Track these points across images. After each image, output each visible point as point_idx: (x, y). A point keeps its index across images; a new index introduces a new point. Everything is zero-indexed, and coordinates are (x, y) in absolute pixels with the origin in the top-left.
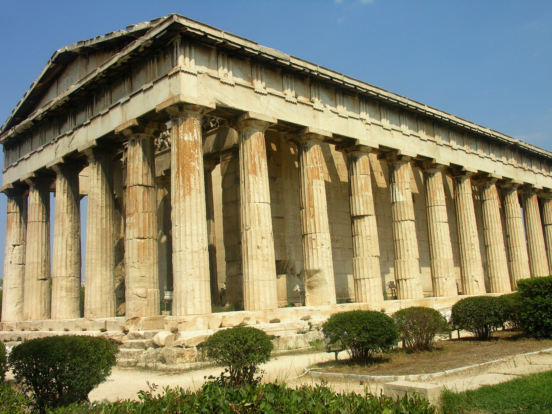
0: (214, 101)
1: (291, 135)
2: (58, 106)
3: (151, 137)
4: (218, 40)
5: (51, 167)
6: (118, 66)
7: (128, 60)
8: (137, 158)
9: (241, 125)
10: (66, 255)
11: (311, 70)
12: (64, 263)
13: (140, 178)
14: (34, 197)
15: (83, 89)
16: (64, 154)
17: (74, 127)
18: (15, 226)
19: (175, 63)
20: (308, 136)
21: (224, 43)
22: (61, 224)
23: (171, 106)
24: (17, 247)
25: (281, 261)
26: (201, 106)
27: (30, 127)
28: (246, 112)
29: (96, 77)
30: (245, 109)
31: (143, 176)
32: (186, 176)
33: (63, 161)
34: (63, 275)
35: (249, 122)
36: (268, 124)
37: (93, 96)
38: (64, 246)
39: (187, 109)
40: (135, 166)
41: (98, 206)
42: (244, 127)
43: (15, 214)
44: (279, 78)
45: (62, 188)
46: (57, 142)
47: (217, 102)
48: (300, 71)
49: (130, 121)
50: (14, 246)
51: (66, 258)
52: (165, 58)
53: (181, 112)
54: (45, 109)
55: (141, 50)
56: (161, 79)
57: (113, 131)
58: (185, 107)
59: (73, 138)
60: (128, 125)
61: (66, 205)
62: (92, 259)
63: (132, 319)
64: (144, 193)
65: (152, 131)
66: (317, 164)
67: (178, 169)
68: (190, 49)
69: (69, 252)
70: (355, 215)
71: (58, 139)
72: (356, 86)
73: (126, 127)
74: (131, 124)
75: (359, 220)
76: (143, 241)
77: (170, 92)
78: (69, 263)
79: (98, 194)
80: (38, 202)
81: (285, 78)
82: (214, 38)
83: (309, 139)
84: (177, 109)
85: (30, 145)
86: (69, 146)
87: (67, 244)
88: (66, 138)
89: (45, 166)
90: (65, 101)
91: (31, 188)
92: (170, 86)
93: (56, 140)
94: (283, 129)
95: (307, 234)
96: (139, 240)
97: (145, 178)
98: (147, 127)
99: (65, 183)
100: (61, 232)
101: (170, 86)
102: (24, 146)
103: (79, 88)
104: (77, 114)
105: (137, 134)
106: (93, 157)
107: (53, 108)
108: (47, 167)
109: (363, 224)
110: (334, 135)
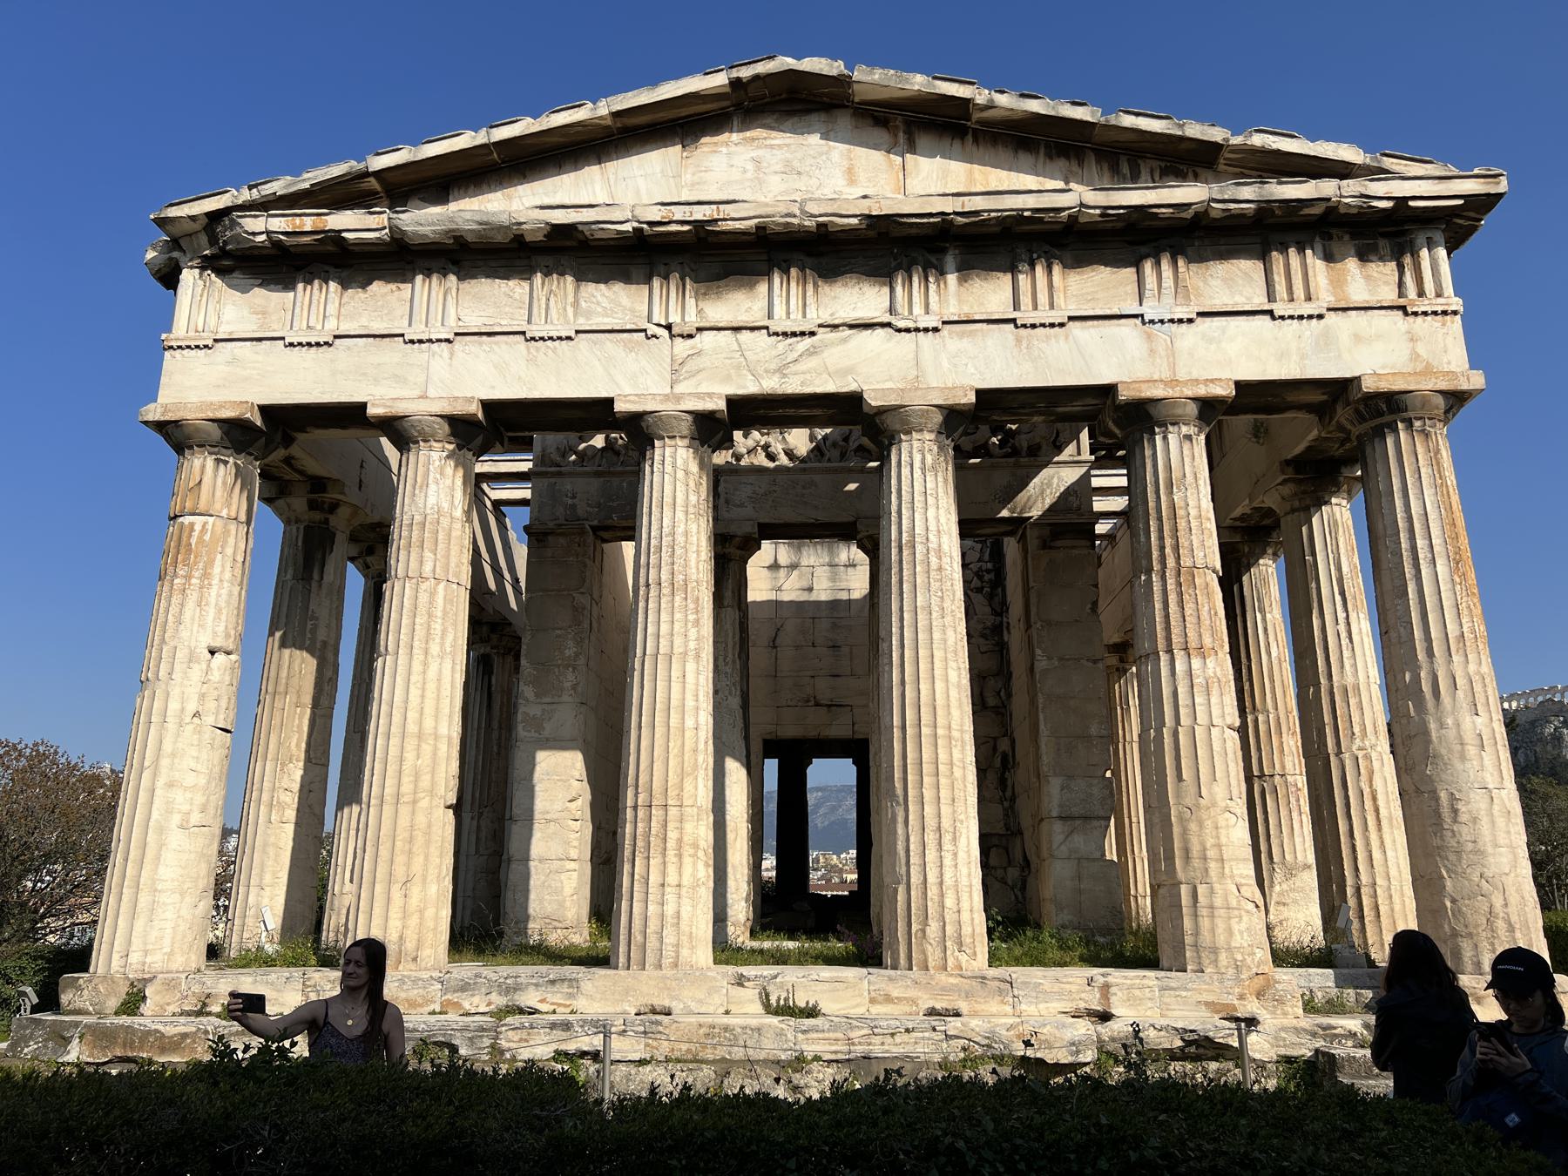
2: (760, 228)
6: (1183, 215)
16: (749, 387)
18: (227, 575)
22: (691, 617)
24: (220, 657)
37: (944, 251)
43: (233, 527)
49: (1212, 381)
50: (212, 653)
54: (679, 213)
55: (1306, 211)
59: (812, 352)
60: (1202, 391)
71: (699, 329)
73: (1190, 393)
77: (1415, 356)
86: (780, 371)
89: (610, 402)
100: (692, 645)
102: (377, 287)
103: (943, 213)
106: (932, 436)
108: (619, 407)
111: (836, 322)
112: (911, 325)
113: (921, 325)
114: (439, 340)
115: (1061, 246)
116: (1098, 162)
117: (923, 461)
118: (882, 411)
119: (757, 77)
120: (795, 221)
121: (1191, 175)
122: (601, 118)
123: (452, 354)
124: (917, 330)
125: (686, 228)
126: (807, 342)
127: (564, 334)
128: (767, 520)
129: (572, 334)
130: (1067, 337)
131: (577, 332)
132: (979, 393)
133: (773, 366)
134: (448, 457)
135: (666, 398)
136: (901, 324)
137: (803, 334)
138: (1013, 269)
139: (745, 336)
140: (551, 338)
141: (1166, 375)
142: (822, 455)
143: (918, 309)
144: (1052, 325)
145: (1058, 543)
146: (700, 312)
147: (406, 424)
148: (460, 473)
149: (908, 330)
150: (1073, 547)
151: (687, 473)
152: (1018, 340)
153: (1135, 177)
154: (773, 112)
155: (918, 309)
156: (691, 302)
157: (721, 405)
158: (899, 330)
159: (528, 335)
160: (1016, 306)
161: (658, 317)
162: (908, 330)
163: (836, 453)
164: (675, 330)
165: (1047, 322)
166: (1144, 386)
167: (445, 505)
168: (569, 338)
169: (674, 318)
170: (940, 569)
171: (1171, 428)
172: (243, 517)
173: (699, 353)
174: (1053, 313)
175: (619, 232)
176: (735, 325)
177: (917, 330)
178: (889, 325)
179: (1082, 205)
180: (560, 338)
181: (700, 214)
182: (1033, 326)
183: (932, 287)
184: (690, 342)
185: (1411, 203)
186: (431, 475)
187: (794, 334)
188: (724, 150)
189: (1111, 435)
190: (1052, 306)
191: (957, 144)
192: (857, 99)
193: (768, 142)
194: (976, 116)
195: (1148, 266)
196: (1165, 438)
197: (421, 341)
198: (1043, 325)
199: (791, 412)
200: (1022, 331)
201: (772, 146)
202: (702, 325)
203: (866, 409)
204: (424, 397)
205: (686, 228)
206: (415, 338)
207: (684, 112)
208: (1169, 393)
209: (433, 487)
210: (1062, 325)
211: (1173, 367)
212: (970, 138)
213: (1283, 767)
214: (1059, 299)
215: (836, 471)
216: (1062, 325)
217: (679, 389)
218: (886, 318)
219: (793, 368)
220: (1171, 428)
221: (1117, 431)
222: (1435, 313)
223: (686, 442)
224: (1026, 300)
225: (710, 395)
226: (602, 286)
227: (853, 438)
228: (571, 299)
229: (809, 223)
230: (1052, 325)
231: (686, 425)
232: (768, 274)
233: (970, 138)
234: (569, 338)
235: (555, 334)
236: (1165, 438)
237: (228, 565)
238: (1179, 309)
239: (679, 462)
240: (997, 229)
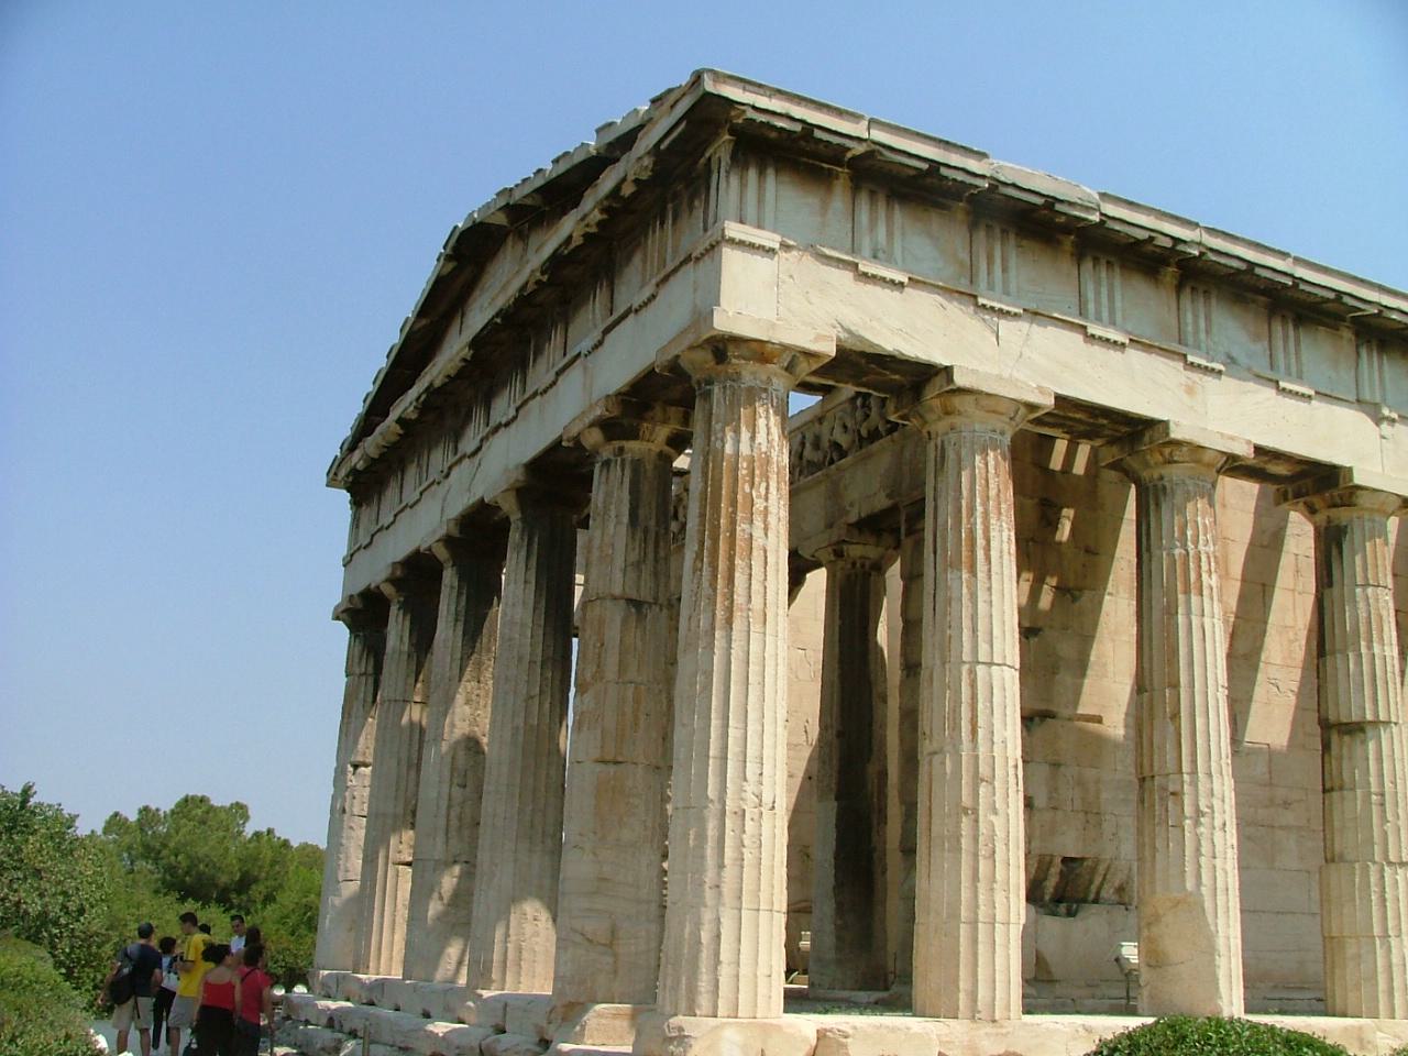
0: (834, 333)
1: (1115, 449)
3: (661, 455)
4: (848, 143)
5: (430, 549)
7: (600, 224)
8: (613, 514)
9: (931, 410)
10: (450, 800)
11: (1177, 240)
12: (442, 822)
13: (618, 575)
14: (397, 631)
17: (484, 431)
19: (711, 220)
20: (1167, 451)
21: (870, 154)
23: (691, 348)
25: (1083, 859)
26: (785, 348)
27: (394, 438)
28: (948, 370)
30: (940, 359)
31: (625, 572)
32: (662, 553)
33: (455, 533)
34: (437, 858)
35: (957, 401)
36: (1023, 410)
38: (447, 773)
39: (735, 357)
40: (606, 539)
41: (520, 659)
42: (940, 419)
43: (364, 678)
44: (1067, 265)
45: (453, 608)
46: (447, 476)
47: (843, 335)
48: (1138, 242)
51: (449, 807)
52: (691, 208)
53: (720, 367)
55: (628, 190)
56: (675, 270)
57: (559, 442)
58: (731, 351)
61: (459, 656)
62: (495, 816)
63: (565, 1006)
64: (625, 622)
65: (663, 432)
66: (1196, 543)
67: (702, 543)
68: (762, 173)
69: (456, 791)
70: (1332, 718)
71: (450, 468)
72: (1340, 294)
73: (587, 421)
74: (598, 412)
75: (1346, 738)
76: (612, 769)
78: (454, 822)
79: (523, 625)
80: (406, 648)
81: (1088, 265)
82: (835, 140)
83: (1170, 462)
84: (710, 356)
85: (397, 491)
87: (453, 770)
88: (466, 462)
90: (464, 360)
91: (394, 609)
92: (695, 290)
93: (446, 471)
94: (1082, 428)
95: (1153, 777)
96: (602, 765)
97: (631, 574)
98: (646, 420)
99: (459, 594)
101: (695, 290)
105: (617, 444)
106: (520, 516)
108: (422, 550)
109: (1358, 749)
110: (1259, 450)
119: (455, 249)
126: (480, 455)
134: (399, 609)
136: (504, 421)
148: (408, 617)
151: (452, 587)
170: (510, 640)
172: (370, 670)
185: (662, 147)
200: (546, 396)
213: (1152, 766)
222: (707, 250)
237: (361, 708)
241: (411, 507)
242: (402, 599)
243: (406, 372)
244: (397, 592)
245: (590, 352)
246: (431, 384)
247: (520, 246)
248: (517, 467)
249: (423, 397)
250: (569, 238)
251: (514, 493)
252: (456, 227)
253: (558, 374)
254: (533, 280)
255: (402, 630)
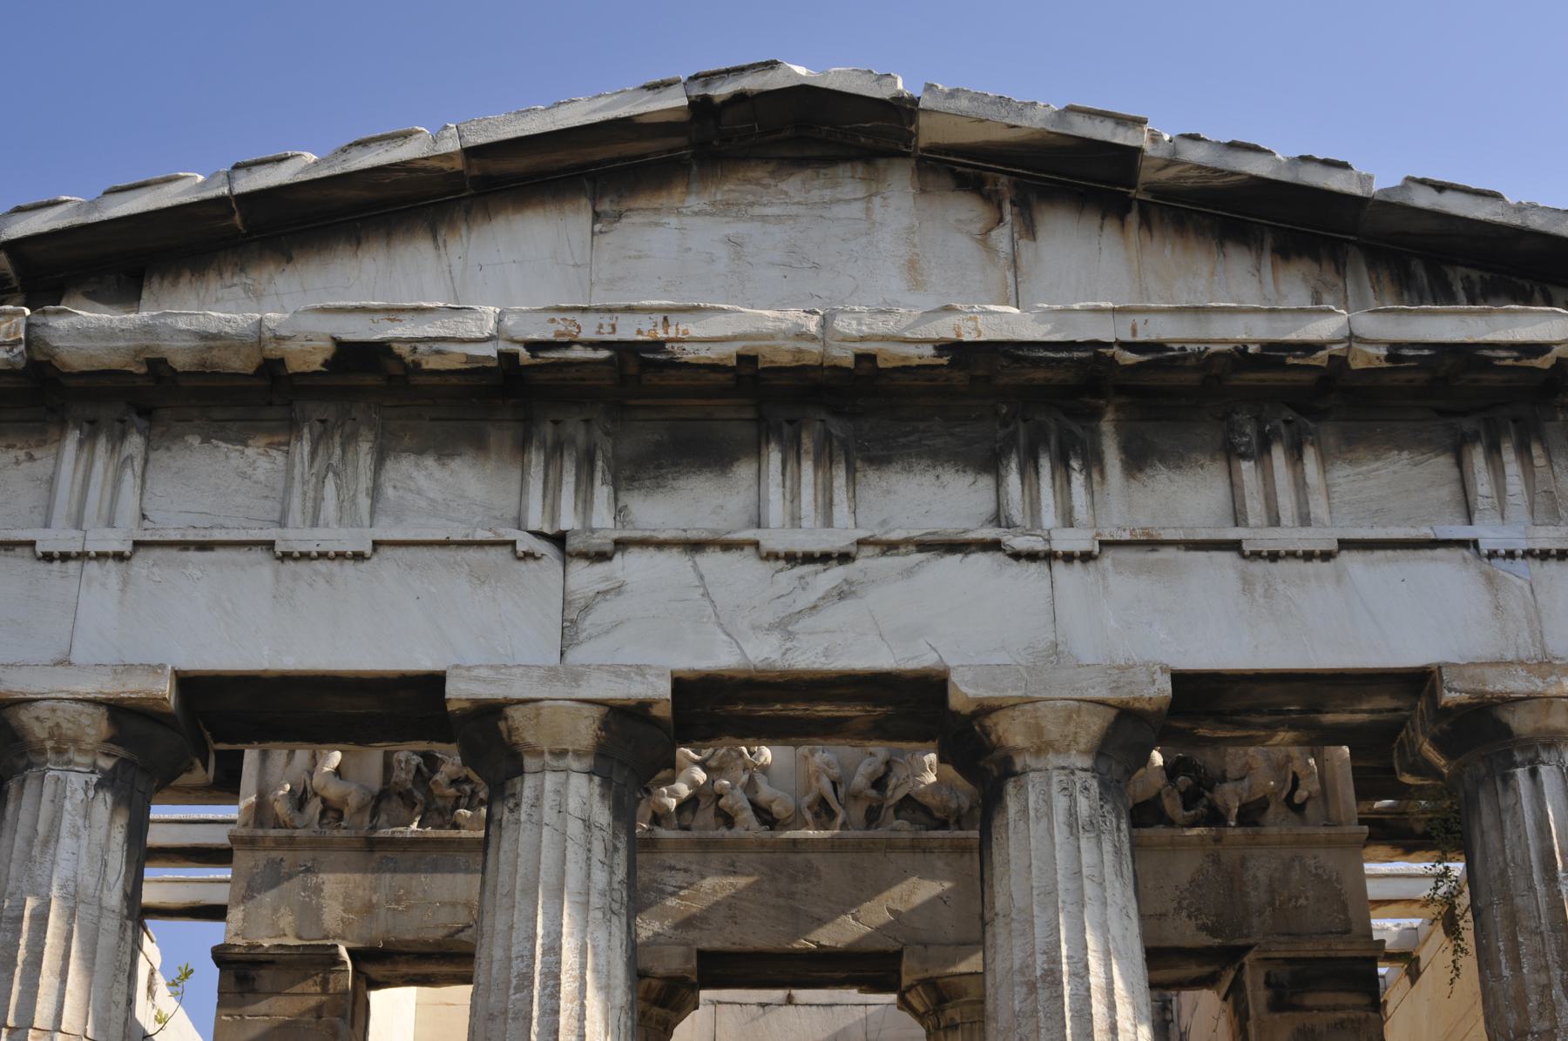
2: (747, 360)
15: (1130, 358)
16: (720, 657)
29: (1310, 348)
37: (1097, 415)
54: (589, 329)
59: (842, 594)
71: (621, 545)
85: (130, 481)
89: (435, 681)
93: (602, 541)
104: (881, 460)
106: (1087, 762)
107: (691, 354)
108: (458, 691)
111: (895, 535)
112: (1039, 545)
113: (1060, 546)
114: (101, 556)
115: (1319, 415)
116: (1372, 266)
117: (1072, 812)
118: (986, 710)
119: (740, 98)
120: (815, 348)
121: (1537, 296)
122: (448, 156)
123: (125, 582)
124: (1049, 557)
125: (603, 354)
126: (835, 574)
127: (349, 549)
128: (717, 944)
129: (368, 549)
130: (1339, 579)
131: (377, 544)
132: (1181, 679)
133: (768, 618)
134: (99, 786)
135: (552, 674)
136: (1021, 543)
137: (825, 558)
138: (1231, 453)
139: (711, 561)
140: (322, 556)
141: (1529, 651)
142: (832, 814)
143: (1049, 517)
144: (1308, 556)
145: (1310, 1000)
146: (620, 512)
147: (25, 716)
149: (1032, 556)
150: (1335, 1009)
151: (588, 824)
152: (1247, 583)
153: (1442, 293)
154: (765, 160)
155: (1049, 517)
156: (602, 493)
157: (664, 690)
158: (1017, 556)
159: (279, 549)
160: (1238, 516)
161: (536, 520)
162: (1032, 556)
163: (858, 812)
164: (573, 544)
165: (1301, 547)
166: (1490, 673)
167: (89, 881)
168: (358, 556)
169: (568, 521)
171: (1544, 756)
173: (619, 590)
174: (1306, 532)
175: (470, 358)
176: (693, 535)
177: (1049, 557)
178: (994, 546)
179: (1352, 337)
180: (340, 556)
181: (628, 329)
182: (1274, 556)
183: (1078, 480)
184: (601, 569)
186: (67, 820)
187: (809, 558)
188: (673, 221)
189: (1423, 768)
190: (1305, 520)
191: (1111, 228)
192: (924, 140)
193: (757, 210)
194: (1146, 175)
195: (1477, 458)
196: (1534, 774)
197: (65, 557)
198: (1292, 555)
199: (798, 709)
201: (764, 218)
202: (626, 534)
203: (954, 702)
204: (65, 662)
205: (603, 354)
206: (56, 548)
207: (600, 153)
208: (1537, 686)
209: (66, 843)
210: (1326, 556)
211: (1539, 636)
212: (1133, 218)
214: (1318, 507)
215: (859, 846)
216: (1326, 556)
217: (576, 656)
218: (989, 533)
219: (807, 622)
220: (1544, 756)
221: (1439, 761)
223: (587, 763)
224: (1255, 506)
225: (640, 670)
226: (430, 462)
227: (893, 782)
228: (365, 482)
229: (843, 355)
230: (1308, 556)
231: (585, 731)
232: (756, 452)
233: (1133, 218)
234: (358, 556)
235: (332, 548)
236: (1534, 774)
238: (1542, 532)
239: (573, 804)
240: (1192, 378)
241: (286, 556)
242: (106, 764)
243: (237, 219)
244: (110, 740)
245: (1511, 555)
246: (658, 345)
247: (966, 210)
248: (1163, 670)
249: (578, 353)
250: (1539, 349)
251: (1111, 714)
252: (771, 65)
253: (1345, 544)
254: (1336, 349)
255: (105, 849)
